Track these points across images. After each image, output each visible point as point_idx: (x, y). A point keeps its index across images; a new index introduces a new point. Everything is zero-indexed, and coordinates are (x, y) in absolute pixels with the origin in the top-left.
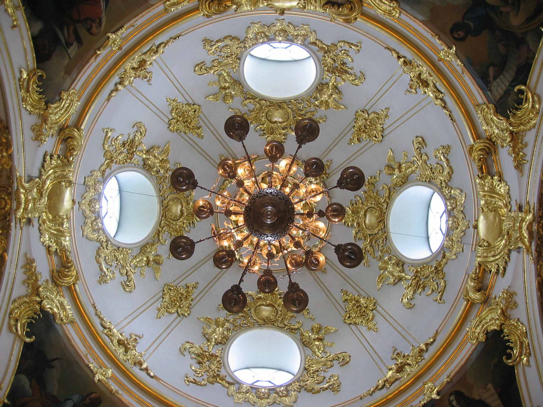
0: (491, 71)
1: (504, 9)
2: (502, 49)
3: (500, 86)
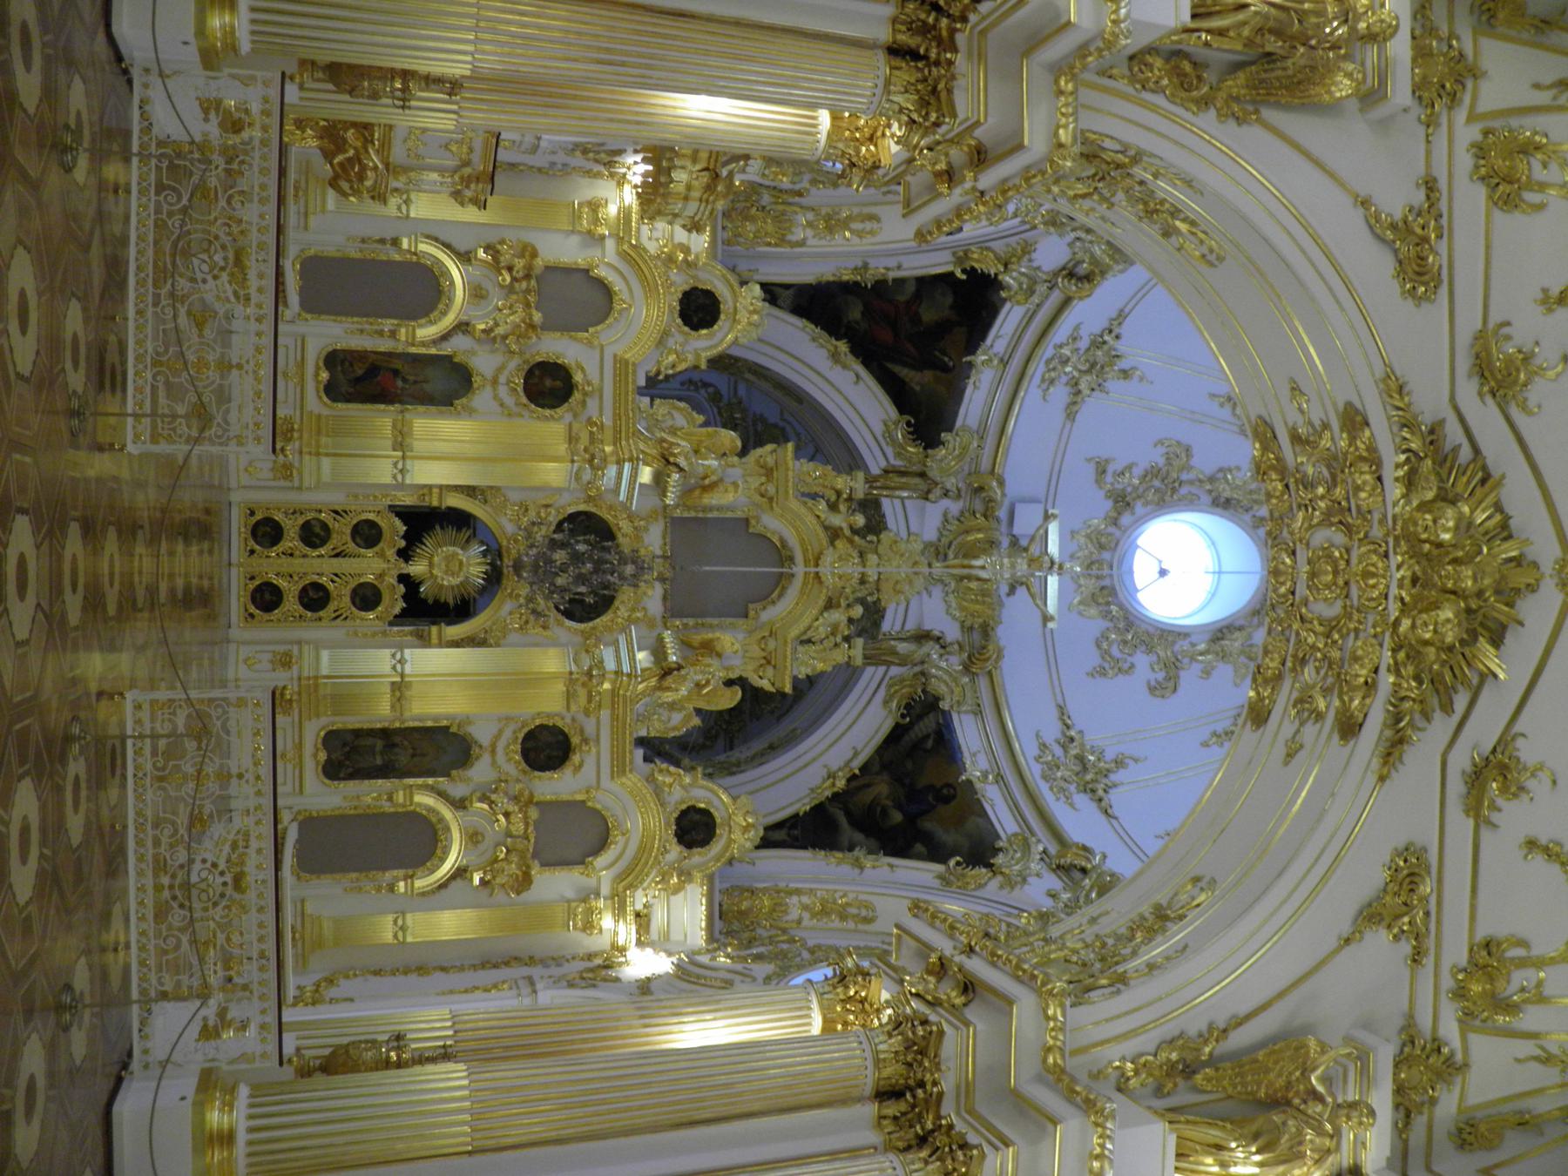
0: (930, 743)
1: (889, 803)
3: (928, 725)
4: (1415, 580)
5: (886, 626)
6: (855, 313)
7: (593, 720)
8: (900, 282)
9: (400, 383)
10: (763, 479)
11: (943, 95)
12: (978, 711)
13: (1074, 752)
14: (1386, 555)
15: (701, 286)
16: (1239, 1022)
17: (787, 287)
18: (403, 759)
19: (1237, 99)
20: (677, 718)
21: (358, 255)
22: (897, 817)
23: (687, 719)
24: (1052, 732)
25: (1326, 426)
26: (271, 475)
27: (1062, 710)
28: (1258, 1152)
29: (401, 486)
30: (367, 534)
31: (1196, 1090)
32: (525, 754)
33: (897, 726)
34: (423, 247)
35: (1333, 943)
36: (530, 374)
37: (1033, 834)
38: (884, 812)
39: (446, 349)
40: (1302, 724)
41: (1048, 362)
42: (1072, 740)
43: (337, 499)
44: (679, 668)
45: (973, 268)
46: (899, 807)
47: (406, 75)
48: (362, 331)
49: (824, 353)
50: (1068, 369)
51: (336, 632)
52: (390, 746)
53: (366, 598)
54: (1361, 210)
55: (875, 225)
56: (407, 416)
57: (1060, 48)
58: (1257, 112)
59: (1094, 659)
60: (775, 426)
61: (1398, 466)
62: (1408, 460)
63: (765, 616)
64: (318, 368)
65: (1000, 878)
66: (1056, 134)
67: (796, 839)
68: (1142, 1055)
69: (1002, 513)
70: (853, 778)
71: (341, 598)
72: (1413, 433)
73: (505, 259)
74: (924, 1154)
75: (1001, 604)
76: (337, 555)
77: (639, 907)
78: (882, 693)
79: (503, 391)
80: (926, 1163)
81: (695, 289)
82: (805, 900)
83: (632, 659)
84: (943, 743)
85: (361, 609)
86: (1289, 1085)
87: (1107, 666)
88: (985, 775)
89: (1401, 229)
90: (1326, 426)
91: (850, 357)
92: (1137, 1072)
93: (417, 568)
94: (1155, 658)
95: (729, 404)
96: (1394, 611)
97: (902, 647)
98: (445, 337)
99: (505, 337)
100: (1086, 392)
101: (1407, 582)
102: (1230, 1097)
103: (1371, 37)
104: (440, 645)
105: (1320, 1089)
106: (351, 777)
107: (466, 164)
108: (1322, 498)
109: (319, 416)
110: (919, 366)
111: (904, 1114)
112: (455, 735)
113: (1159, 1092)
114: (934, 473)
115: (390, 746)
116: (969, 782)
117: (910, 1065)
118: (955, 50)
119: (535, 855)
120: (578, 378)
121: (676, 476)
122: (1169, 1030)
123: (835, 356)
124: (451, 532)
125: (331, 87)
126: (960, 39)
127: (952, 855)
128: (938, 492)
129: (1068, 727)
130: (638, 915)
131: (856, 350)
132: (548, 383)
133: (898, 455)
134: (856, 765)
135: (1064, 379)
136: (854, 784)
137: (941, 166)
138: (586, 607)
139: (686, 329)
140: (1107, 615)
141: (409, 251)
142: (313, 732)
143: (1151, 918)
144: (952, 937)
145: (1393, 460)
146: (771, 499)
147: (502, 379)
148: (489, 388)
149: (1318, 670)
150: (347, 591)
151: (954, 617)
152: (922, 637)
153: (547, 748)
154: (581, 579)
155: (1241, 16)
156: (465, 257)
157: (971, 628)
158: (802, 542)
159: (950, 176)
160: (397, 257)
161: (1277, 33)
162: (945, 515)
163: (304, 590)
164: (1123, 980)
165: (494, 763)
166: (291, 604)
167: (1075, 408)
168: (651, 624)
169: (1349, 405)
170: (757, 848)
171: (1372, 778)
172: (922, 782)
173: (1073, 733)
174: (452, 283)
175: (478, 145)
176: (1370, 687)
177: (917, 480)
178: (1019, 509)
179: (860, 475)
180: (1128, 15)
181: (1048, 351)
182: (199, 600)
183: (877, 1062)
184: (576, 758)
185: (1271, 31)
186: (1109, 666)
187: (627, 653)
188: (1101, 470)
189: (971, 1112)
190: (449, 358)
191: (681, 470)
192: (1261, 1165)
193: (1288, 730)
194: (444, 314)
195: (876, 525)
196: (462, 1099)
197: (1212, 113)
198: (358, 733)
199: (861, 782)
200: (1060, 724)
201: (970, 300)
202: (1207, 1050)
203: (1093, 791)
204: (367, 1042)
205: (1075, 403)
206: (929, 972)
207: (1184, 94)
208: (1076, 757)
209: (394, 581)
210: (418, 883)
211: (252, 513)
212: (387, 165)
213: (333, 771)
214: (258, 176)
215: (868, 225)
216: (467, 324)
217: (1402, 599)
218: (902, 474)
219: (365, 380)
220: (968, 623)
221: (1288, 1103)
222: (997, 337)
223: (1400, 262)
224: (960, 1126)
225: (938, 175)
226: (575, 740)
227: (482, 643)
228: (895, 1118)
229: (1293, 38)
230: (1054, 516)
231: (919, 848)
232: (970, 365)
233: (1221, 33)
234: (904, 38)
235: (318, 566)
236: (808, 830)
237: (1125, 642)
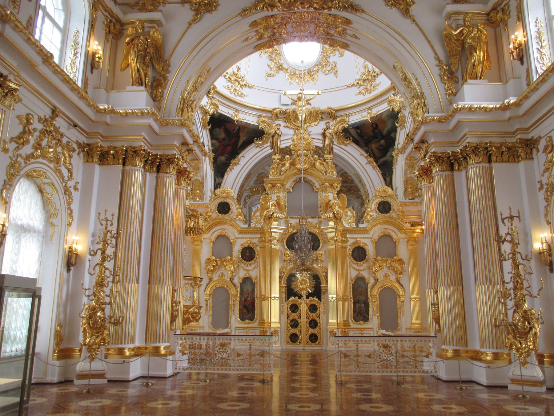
0: (359, 131)
1: (378, 144)
2: (366, 138)
3: (353, 132)
4: (302, 3)
5: (321, 145)
6: (222, 158)
7: (350, 239)
8: (213, 145)
9: (249, 299)
11: (169, 157)
12: (349, 115)
13: (362, 83)
14: (295, 13)
15: (216, 208)
16: (437, 58)
17: (215, 180)
18: (362, 298)
19: (163, 68)
20: (349, 214)
21: (211, 311)
22: (382, 142)
23: (350, 210)
24: (355, 90)
25: (256, 31)
26: (277, 337)
27: (348, 87)
28: (476, 53)
29: (280, 298)
30: (294, 308)
31: (457, 70)
32: (361, 260)
33: (353, 141)
35: (414, 25)
37: (388, 98)
38: (381, 146)
39: (238, 285)
40: (347, 34)
41: (236, 96)
42: (358, 83)
43: (284, 317)
44: (334, 213)
45: (208, 123)
46: (379, 141)
47: (172, 303)
49: (235, 168)
50: (238, 89)
51: (323, 317)
52: (358, 301)
53: (313, 308)
54: (193, 25)
56: (258, 296)
57: (156, 127)
58: (166, 61)
59: (331, 75)
60: (257, 177)
61: (268, 10)
62: (266, 7)
63: (318, 186)
64: (245, 323)
65: (402, 110)
66: (179, 126)
67: (389, 174)
68: (445, 88)
69: (284, 108)
70: (370, 155)
71: (313, 315)
72: (257, 7)
73: (212, 268)
74: (468, 158)
75: (314, 108)
76: (301, 317)
77: (409, 225)
78: (343, 147)
79: (250, 268)
80: (471, 158)
81: (218, 210)
82: (408, 172)
83: (331, 228)
84: (359, 127)
85: (317, 310)
86: (457, 40)
87: (334, 71)
88: (369, 113)
89: (197, 12)
90: (256, 31)
91: (236, 159)
92: (450, 90)
93: (304, 294)
94: (331, 55)
95: (251, 192)
96: (312, 9)
97: (327, 142)
98: (235, 285)
100: (245, 82)
101: (303, 6)
102: (460, 59)
103: (143, 28)
104: (327, 287)
105: (458, 31)
106: (368, 314)
107: (191, 284)
108: (278, 30)
109: (259, 323)
110: (239, 137)
111: (458, 163)
112: (355, 282)
113: (457, 82)
114: (273, 132)
115: (358, 301)
116: (371, 118)
117: (443, 161)
118: (157, 155)
119: (392, 258)
120: (246, 245)
122: (438, 79)
124: (293, 283)
125: (174, 323)
126: (154, 152)
127: (395, 125)
128: (278, 132)
129: (354, 84)
130: (412, 226)
133: (267, 143)
134: (366, 155)
135: (241, 90)
136: (372, 155)
137: (187, 152)
138: (315, 242)
140: (317, 71)
142: (353, 325)
143: (405, 82)
144: (409, 144)
145: (266, 13)
146: (281, 185)
147: (247, 268)
148: (250, 272)
149: (330, 29)
150: (312, 315)
151: (318, 123)
152: (324, 135)
153: (359, 254)
154: (306, 246)
155: (141, 71)
157: (322, 118)
158: (295, 175)
159: (190, 151)
160: (211, 300)
161: (144, 58)
162: (285, 127)
163: (311, 327)
164: (422, 94)
165: (363, 270)
166: (315, 331)
167: (250, 86)
168: (320, 222)
169: (250, 26)
170: (392, 188)
171: (363, 15)
172: (372, 135)
173: (356, 83)
175: (186, 282)
176: (335, 16)
177: (275, 139)
178: (282, 103)
179: (273, 157)
180: (146, 109)
181: (232, 96)
182: (315, 359)
183: (442, 171)
184: (362, 245)
185: (144, 60)
186: (334, 70)
187: (330, 229)
188: (270, 75)
189: (458, 142)
190: (241, 284)
191: (273, 213)
192: (480, 52)
193: (349, 38)
195: (287, 151)
196: (450, 289)
197: (167, 75)
198: (354, 312)
199: (370, 151)
200: (353, 88)
201: (217, 122)
202: (445, 67)
203: (375, 76)
204: (433, 313)
205: (249, 86)
206: (419, 151)
207: (163, 84)
208: (363, 82)
209: (308, 300)
210: (401, 293)
211: (288, 342)
212: (193, 306)
213: (366, 319)
214: (196, 340)
217: (308, 7)
218: (273, 143)
219: (248, 309)
220: (320, 119)
221: (463, 40)
222: (229, 113)
223: (207, 12)
224: (461, 147)
225: (189, 153)
226: (357, 245)
227: (327, 273)
228: (459, 165)
229: (145, 53)
230: (285, 93)
231: (392, 135)
232: (237, 121)
233: (146, 75)
234: (155, 169)
235: (304, 323)
236: (386, 169)
237: (326, 65)
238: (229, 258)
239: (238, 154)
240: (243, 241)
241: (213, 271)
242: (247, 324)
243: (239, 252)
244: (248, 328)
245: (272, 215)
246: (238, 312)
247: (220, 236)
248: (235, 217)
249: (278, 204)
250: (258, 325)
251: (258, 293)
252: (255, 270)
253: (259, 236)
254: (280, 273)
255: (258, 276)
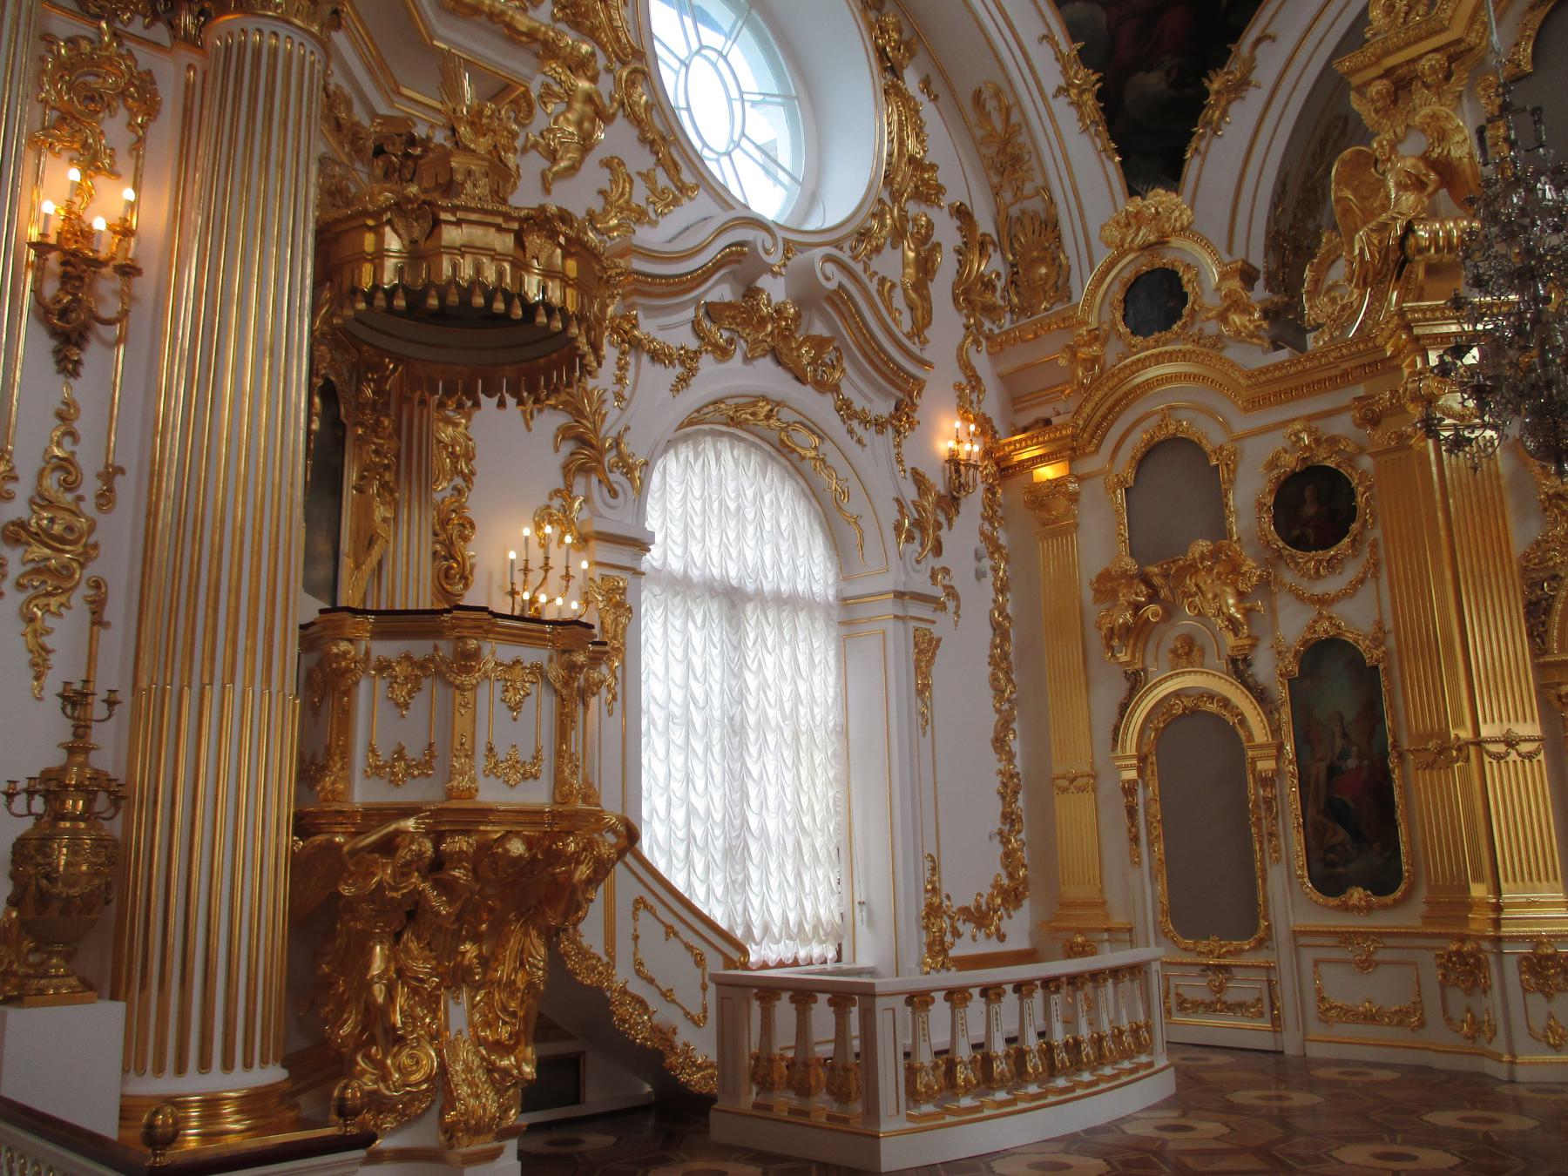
6: (1153, 82)
9: (1351, 763)
10: (1416, 85)
21: (1159, 848)
34: (1131, 749)
36: (1299, 543)
39: (1282, 693)
48: (1271, 834)
49: (1235, 108)
55: (986, 95)
56: (1405, 744)
64: (1346, 908)
79: (1331, 585)
98: (1261, 696)
99: (1240, 595)
120: (1290, 462)
121: (1422, 233)
123: (1240, 87)
131: (1219, 59)
132: (1310, 510)
139: (1186, 311)
141: (1141, 771)
146: (1451, 59)
147: (1319, 589)
148: (1336, 610)
156: (1136, 682)
174: (1177, 694)
191: (1409, 229)
194: (1226, 703)
215: (991, 105)
216: (1234, 661)
238: (1202, 546)
239: (1236, 34)
240: (1278, 441)
241: (1137, 632)
242: (1357, 912)
243: (1261, 505)
244: (1366, 935)
245: (1403, 239)
246: (1296, 843)
247: (1150, 454)
248: (1211, 328)
249: (1446, 171)
250: (1426, 918)
251: (1406, 717)
252: (1366, 593)
253: (1361, 391)
254: (1534, 585)
255: (1389, 625)
